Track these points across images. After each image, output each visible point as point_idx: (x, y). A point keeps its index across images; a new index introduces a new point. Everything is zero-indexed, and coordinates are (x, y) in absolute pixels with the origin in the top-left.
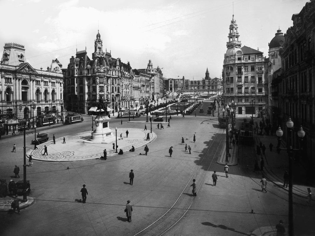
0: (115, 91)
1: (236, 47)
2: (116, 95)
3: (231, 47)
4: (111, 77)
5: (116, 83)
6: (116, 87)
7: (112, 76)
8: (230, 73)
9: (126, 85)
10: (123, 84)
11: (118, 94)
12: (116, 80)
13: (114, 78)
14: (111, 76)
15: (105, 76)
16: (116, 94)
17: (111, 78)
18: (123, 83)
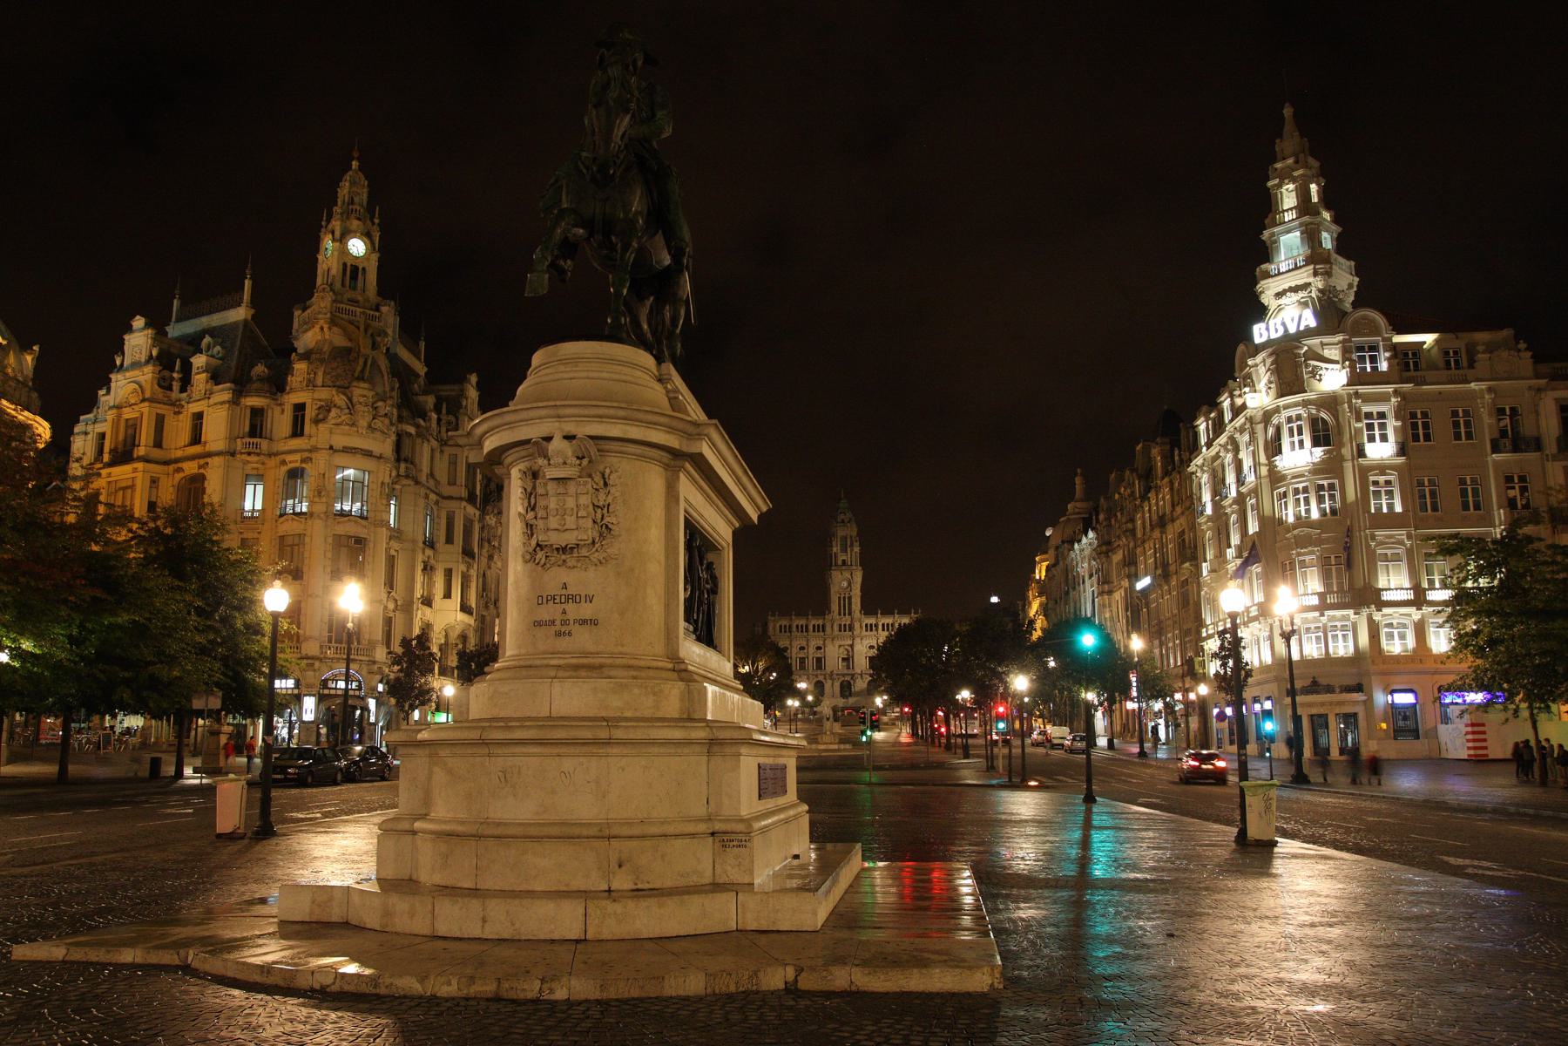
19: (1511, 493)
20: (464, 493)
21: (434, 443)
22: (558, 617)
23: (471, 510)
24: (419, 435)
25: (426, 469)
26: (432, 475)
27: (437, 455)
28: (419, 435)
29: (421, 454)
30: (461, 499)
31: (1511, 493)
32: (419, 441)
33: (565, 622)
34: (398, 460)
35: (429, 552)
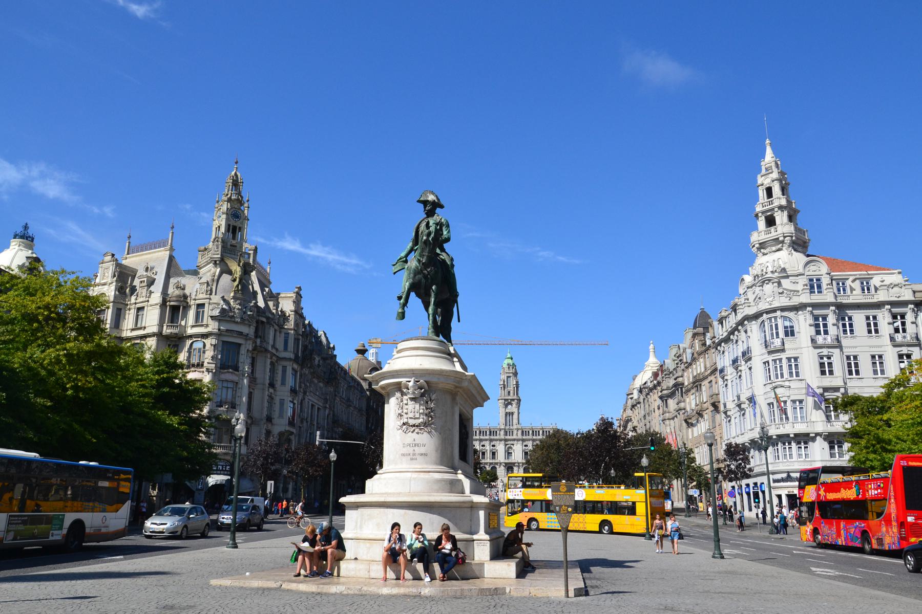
0: (276, 415)
1: (795, 250)
2: (281, 434)
3: (774, 248)
4: (266, 350)
5: (283, 383)
6: (282, 402)
7: (274, 351)
8: (783, 344)
9: (313, 405)
10: (306, 400)
11: (288, 428)
12: (284, 368)
13: (279, 359)
14: (270, 349)
15: (246, 337)
16: (282, 429)
17: (269, 361)
18: (305, 393)
19: (902, 365)
20: (292, 356)
21: (276, 327)
22: (412, 452)
23: (295, 366)
24: (268, 323)
25: (271, 342)
26: (273, 346)
27: (278, 333)
28: (268, 323)
29: (269, 333)
30: (290, 359)
31: (902, 365)
32: (267, 326)
33: (414, 455)
34: (256, 337)
35: (271, 390)
